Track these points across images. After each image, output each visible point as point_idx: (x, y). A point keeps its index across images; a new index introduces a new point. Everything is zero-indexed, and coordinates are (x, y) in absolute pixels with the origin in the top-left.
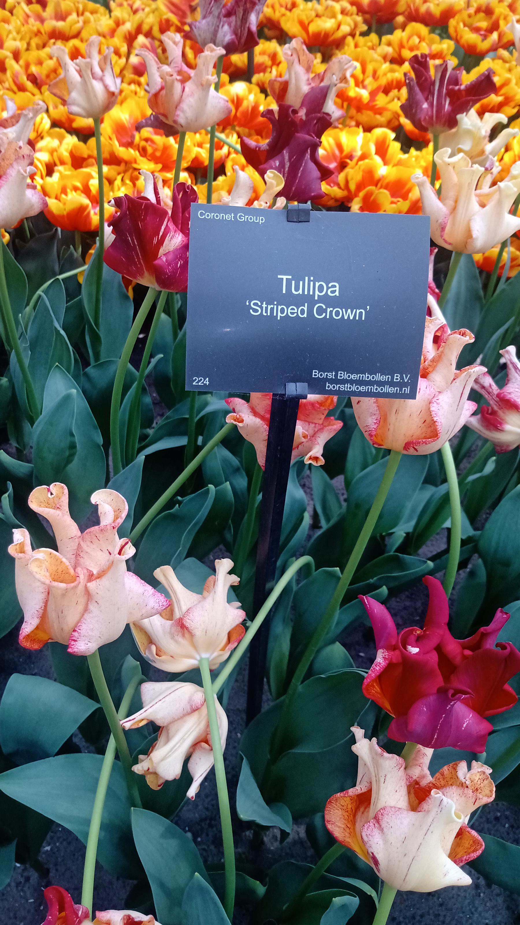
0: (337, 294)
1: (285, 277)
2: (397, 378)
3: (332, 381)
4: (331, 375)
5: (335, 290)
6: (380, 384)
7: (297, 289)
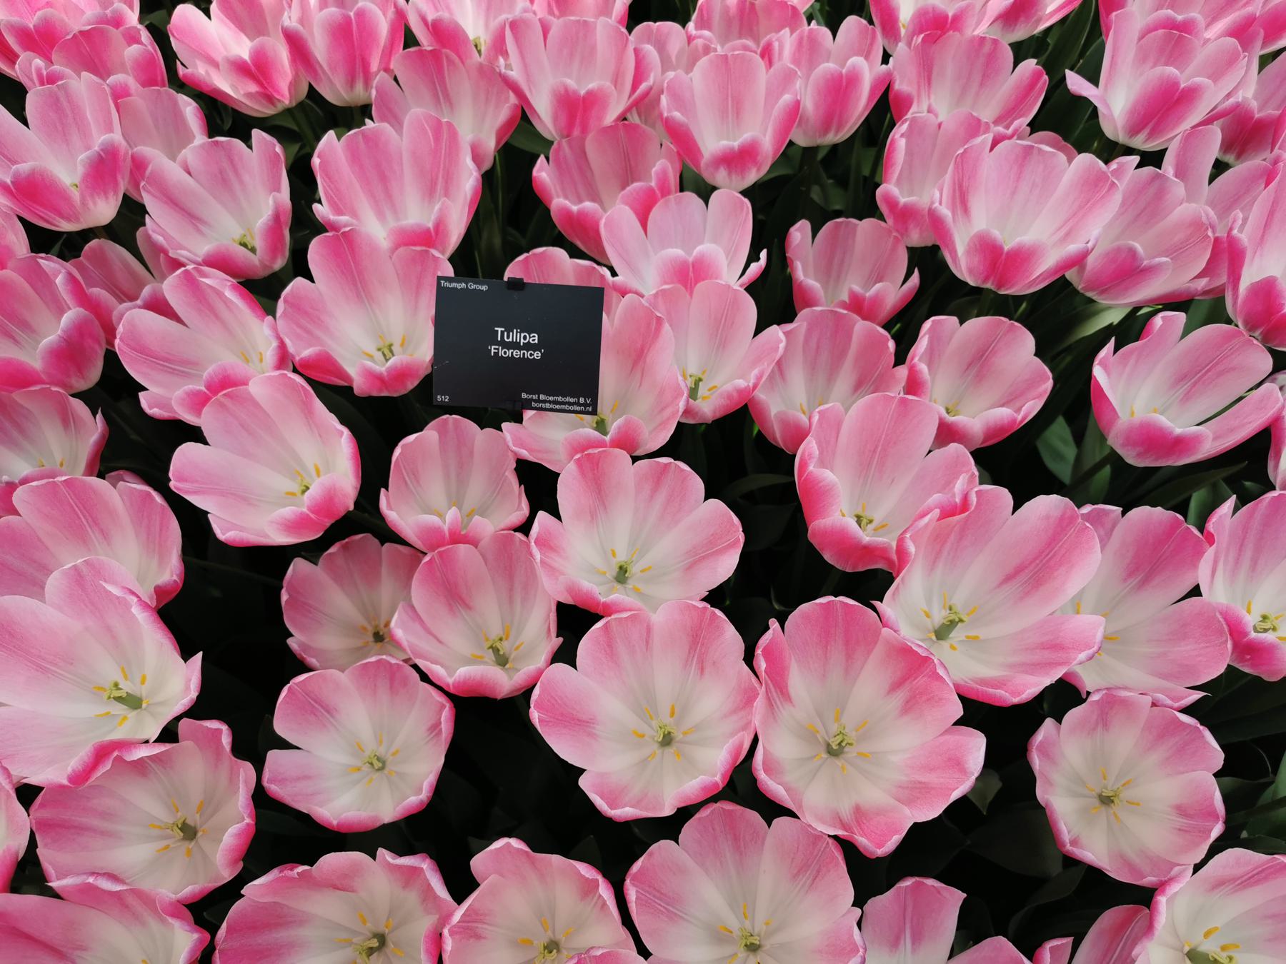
1: (500, 330)
3: (536, 401)
4: (535, 397)
5: (534, 339)
6: (570, 404)
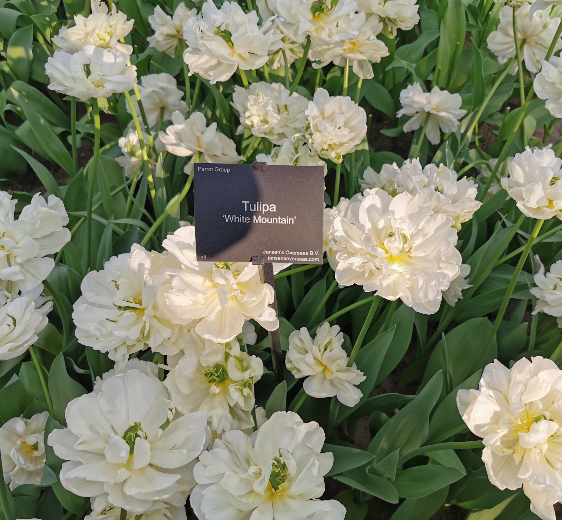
0: (275, 210)
2: (311, 253)
7: (253, 209)
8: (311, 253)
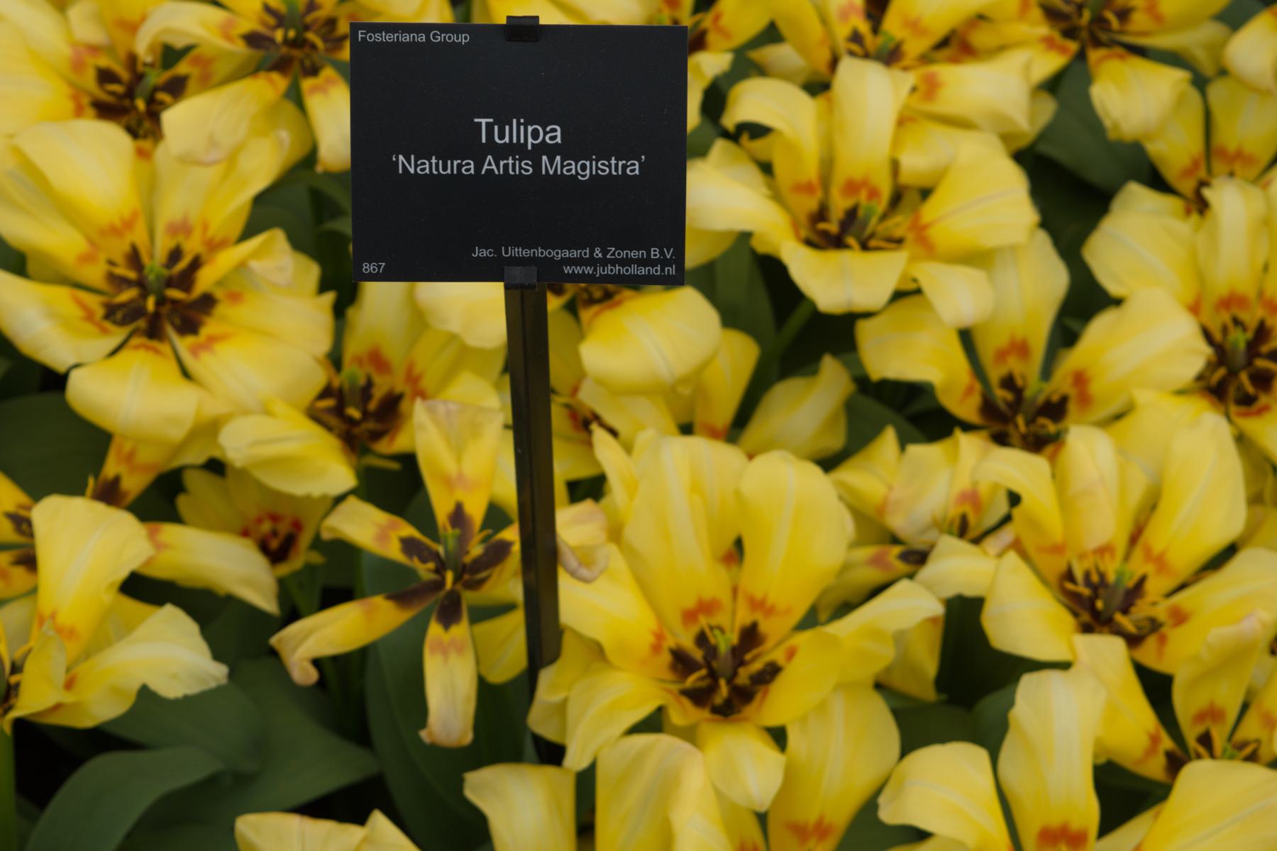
0: (559, 140)
1: (484, 121)
7: (502, 136)
8: (655, 253)
